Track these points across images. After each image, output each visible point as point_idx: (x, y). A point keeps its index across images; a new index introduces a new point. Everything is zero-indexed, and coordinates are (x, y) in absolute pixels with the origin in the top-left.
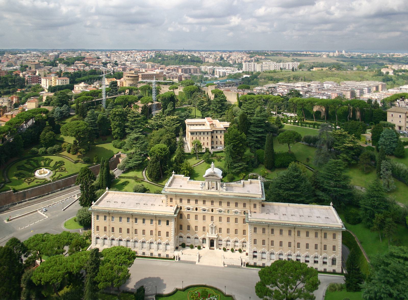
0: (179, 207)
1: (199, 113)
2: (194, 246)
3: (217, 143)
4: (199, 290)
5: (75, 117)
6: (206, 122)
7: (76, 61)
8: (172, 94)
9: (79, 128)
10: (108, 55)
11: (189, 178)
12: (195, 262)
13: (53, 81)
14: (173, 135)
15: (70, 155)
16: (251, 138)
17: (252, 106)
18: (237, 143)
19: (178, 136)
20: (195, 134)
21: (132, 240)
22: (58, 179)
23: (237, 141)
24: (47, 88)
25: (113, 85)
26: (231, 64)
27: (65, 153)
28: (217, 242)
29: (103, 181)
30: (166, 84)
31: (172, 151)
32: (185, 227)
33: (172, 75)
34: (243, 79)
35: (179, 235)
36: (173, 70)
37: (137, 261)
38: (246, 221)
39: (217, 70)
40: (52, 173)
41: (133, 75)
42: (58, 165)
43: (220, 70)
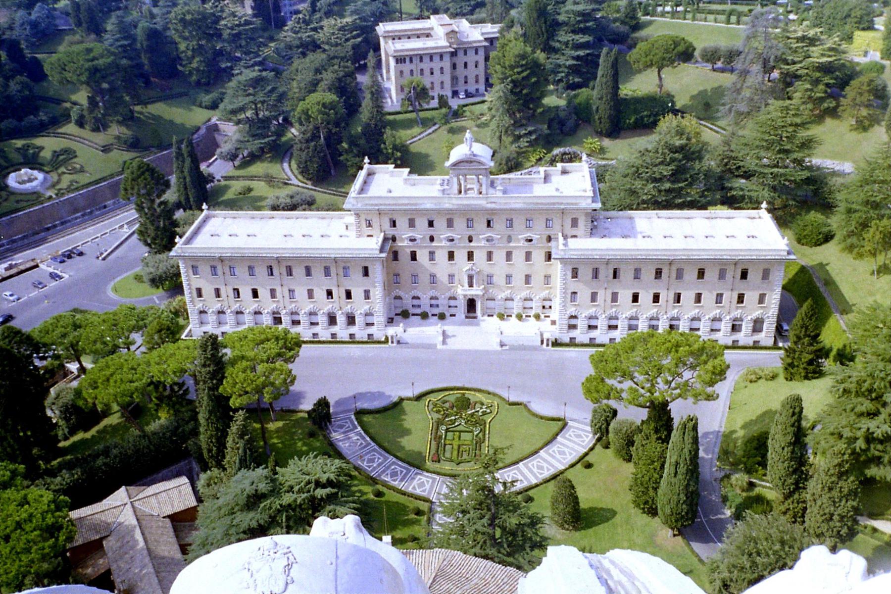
0: (390, 236)
2: (430, 315)
3: (466, 82)
4: (452, 397)
6: (435, 28)
9: (96, 62)
11: (406, 170)
12: (435, 345)
14: (347, 67)
15: (86, 133)
19: (363, 68)
20: (408, 60)
21: (284, 311)
22: (69, 190)
23: (522, 72)
27: (71, 128)
31: (353, 108)
32: (405, 277)
35: (394, 294)
37: (303, 346)
38: (553, 256)
42: (62, 157)
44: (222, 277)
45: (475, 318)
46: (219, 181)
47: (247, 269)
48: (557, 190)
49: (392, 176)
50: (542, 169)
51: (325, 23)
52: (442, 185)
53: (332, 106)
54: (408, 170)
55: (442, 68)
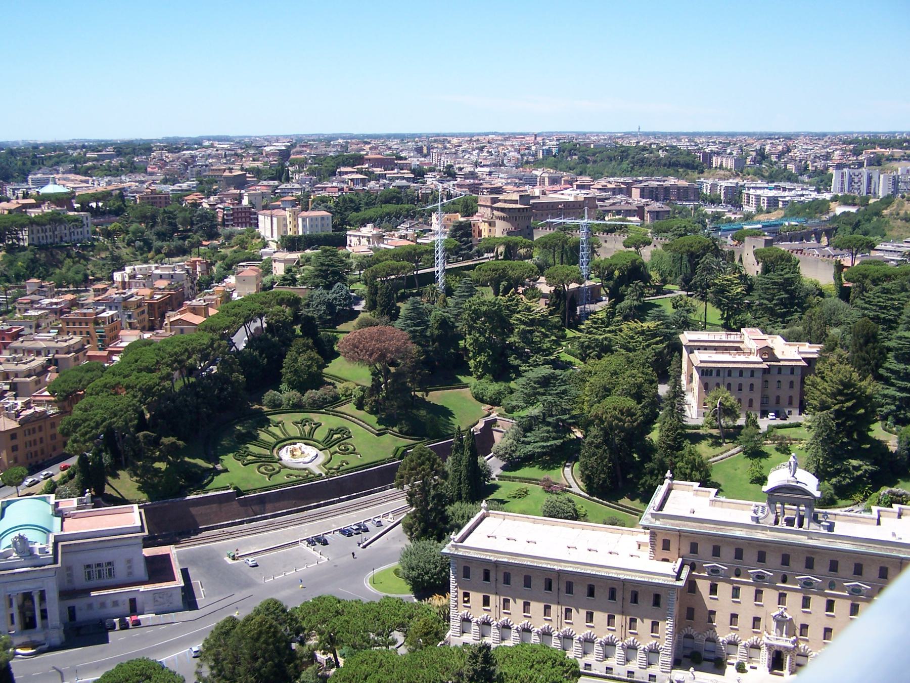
1: (715, 314)
5: (367, 315)
7: (338, 165)
8: (635, 260)
10: (422, 148)
13: (289, 220)
14: (647, 374)
16: (886, 392)
17: (892, 299)
18: (849, 404)
20: (714, 373)
24: (276, 238)
25: (459, 233)
26: (792, 174)
28: (791, 659)
29: (460, 483)
30: (611, 230)
33: (614, 204)
34: (835, 218)
36: (615, 191)
39: (752, 191)
40: (323, 457)
41: (514, 206)
43: (759, 192)
44: (493, 585)
45: (782, 675)
46: (494, 479)
47: (523, 579)
48: (894, 535)
49: (696, 495)
50: (875, 509)
51: (624, 326)
52: (755, 512)
53: (630, 413)
54: (716, 490)
55: (752, 385)
